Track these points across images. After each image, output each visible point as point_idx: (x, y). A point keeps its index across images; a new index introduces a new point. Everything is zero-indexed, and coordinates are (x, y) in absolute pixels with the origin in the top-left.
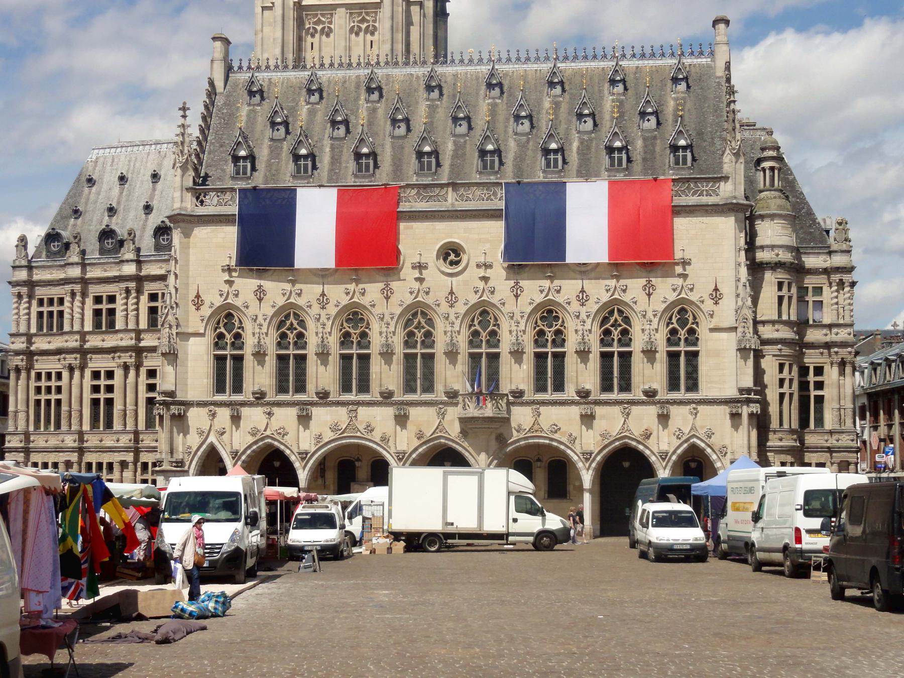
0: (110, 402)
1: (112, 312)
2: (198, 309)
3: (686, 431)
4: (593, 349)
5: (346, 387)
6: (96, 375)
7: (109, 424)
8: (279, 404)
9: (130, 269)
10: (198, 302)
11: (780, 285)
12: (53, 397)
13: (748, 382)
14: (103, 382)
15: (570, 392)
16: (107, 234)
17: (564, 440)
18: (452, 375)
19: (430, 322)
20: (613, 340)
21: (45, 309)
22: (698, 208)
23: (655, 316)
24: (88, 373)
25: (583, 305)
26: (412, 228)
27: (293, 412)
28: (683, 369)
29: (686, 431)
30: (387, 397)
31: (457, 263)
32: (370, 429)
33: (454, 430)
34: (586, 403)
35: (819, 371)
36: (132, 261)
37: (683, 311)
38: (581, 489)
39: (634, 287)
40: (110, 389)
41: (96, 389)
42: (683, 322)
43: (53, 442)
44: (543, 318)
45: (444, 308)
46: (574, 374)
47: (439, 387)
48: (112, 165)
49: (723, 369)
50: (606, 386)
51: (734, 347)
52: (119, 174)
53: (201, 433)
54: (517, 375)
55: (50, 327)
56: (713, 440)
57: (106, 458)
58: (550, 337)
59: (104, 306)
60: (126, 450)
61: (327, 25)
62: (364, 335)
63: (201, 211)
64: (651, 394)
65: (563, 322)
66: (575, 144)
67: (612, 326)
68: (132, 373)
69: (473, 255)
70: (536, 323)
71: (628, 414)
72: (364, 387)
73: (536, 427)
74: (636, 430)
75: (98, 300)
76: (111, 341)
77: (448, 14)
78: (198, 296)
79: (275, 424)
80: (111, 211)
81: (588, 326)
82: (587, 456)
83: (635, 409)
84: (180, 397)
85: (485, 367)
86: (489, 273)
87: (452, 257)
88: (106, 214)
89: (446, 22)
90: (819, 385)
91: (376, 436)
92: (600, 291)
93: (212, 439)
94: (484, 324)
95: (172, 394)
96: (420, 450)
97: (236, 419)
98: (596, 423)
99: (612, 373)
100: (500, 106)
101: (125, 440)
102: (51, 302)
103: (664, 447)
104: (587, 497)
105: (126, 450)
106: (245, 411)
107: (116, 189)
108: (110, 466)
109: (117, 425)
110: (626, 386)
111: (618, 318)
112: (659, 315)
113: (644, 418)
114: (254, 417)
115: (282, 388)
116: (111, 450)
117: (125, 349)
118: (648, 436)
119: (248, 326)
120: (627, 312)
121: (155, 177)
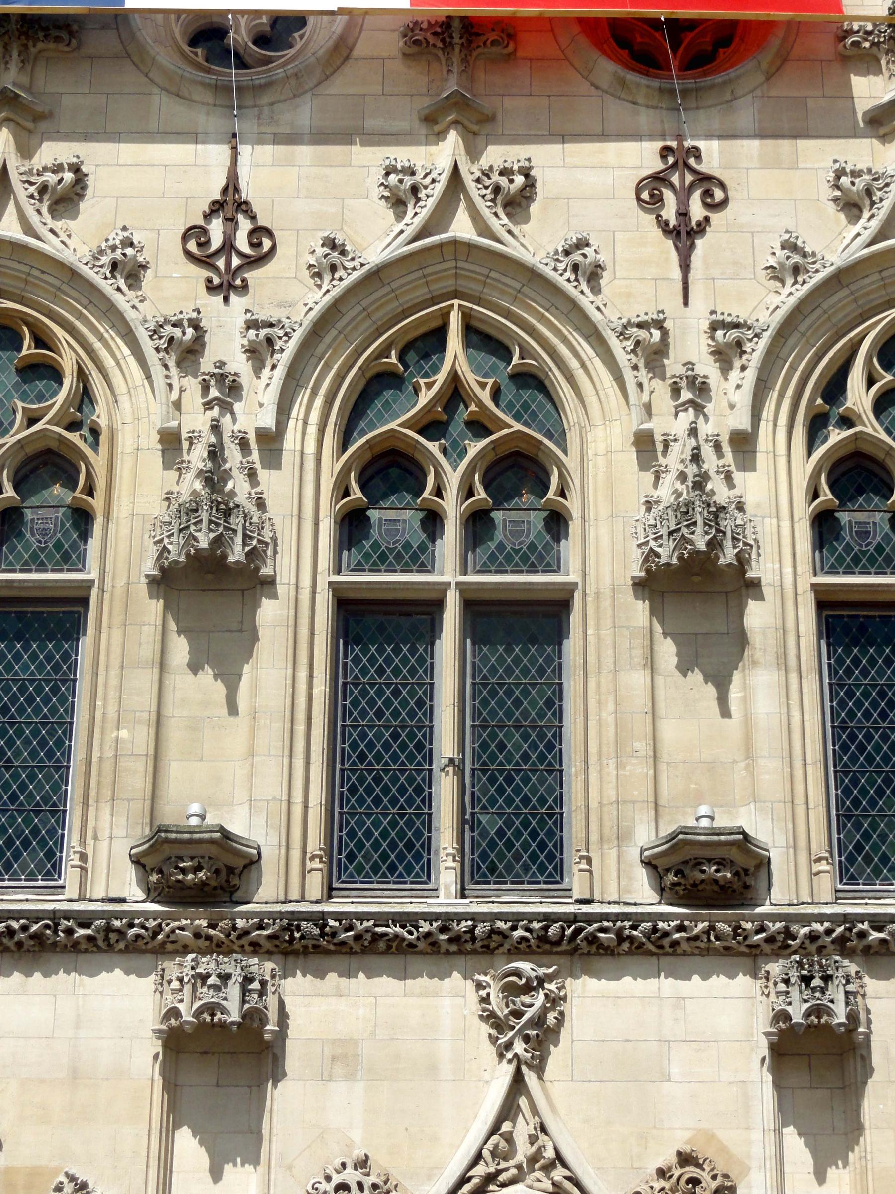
4: (283, 567)
20: (433, 521)
23: (726, 356)
25: (226, 287)
34: (210, 946)
39: (585, 186)
46: (136, 737)
65: (85, 396)
67: (432, 427)
71: (543, 1035)
81: (256, 410)
92: (336, 200)
98: (288, 1104)
99: (421, 746)
111: (470, 378)
112: (757, 350)
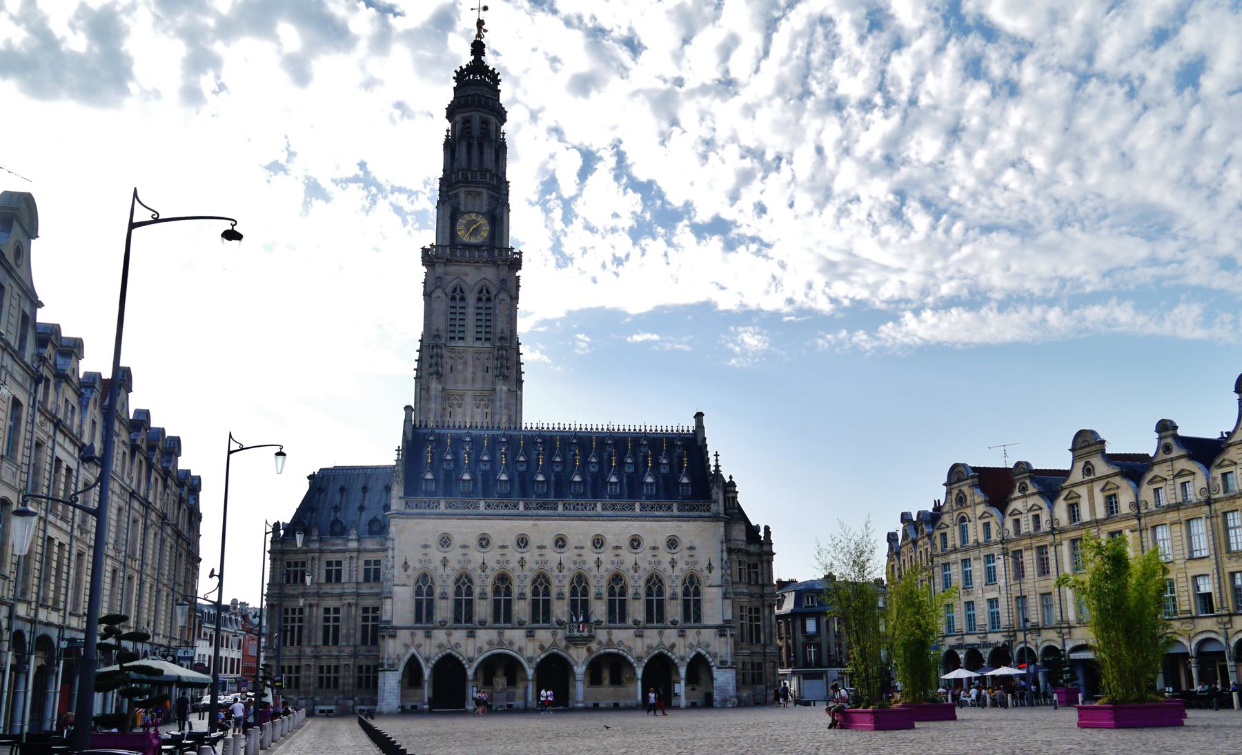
0: (336, 629)
1: (339, 572)
3: (695, 643)
5: (496, 618)
6: (327, 610)
7: (336, 642)
8: (456, 629)
9: (353, 545)
10: (406, 566)
11: (740, 562)
12: (297, 624)
13: (729, 616)
14: (332, 615)
15: (630, 622)
16: (336, 522)
19: (548, 581)
21: (292, 569)
24: (321, 611)
27: (463, 633)
29: (695, 643)
30: (521, 624)
31: (563, 546)
32: (511, 643)
33: (564, 643)
35: (757, 610)
37: (692, 576)
38: (633, 678)
40: (336, 619)
41: (327, 619)
43: (296, 653)
45: (556, 572)
47: (554, 619)
49: (715, 608)
50: (649, 619)
51: (720, 595)
53: (407, 646)
55: (295, 581)
56: (710, 649)
57: (333, 663)
58: (617, 590)
59: (334, 568)
60: (350, 657)
62: (508, 588)
63: (408, 511)
64: (674, 623)
66: (625, 480)
68: (353, 609)
69: (572, 541)
72: (508, 619)
74: (667, 645)
75: (329, 564)
76: (337, 589)
79: (453, 641)
80: (336, 509)
82: (639, 659)
83: (667, 631)
84: (395, 623)
85: (579, 606)
86: (582, 552)
90: (757, 619)
91: (516, 647)
93: (413, 650)
95: (390, 622)
96: (543, 656)
97: (428, 636)
101: (348, 650)
102: (296, 564)
103: (682, 654)
104: (639, 683)
105: (350, 657)
106: (435, 632)
107: (338, 497)
108: (337, 668)
109: (342, 642)
110: (661, 619)
113: (671, 635)
114: (440, 635)
115: (457, 619)
116: (338, 658)
117: (351, 594)
118: (673, 646)
119: (438, 582)
120: (662, 575)
121: (365, 489)
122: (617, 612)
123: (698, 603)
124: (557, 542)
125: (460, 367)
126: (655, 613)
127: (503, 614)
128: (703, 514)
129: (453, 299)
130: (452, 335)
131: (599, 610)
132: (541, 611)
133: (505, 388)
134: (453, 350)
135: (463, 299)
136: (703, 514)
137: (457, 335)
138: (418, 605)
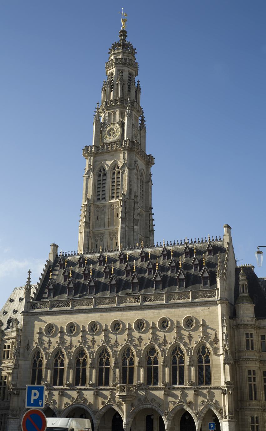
2: (28, 350)
17: (157, 406)
18: (116, 374)
22: (207, 303)
26: (103, 315)
28: (205, 374)
36: (15, 331)
42: (204, 352)
44: (150, 352)
48: (19, 294)
52: (19, 298)
54: (140, 376)
61: (101, 238)
70: (147, 354)
73: (146, 401)
77: (154, 230)
78: (28, 345)
87: (117, 327)
88: (13, 313)
89: (153, 234)
94: (128, 355)
100: (145, 265)
122: (152, 376)
123: (208, 368)
124: (115, 325)
125: (103, 216)
126: (178, 376)
127: (80, 378)
128: (210, 299)
129: (100, 175)
130: (98, 197)
131: (140, 376)
132: (103, 377)
133: (124, 226)
134: (98, 207)
135: (105, 175)
136: (210, 299)
137: (101, 197)
138: (34, 371)
